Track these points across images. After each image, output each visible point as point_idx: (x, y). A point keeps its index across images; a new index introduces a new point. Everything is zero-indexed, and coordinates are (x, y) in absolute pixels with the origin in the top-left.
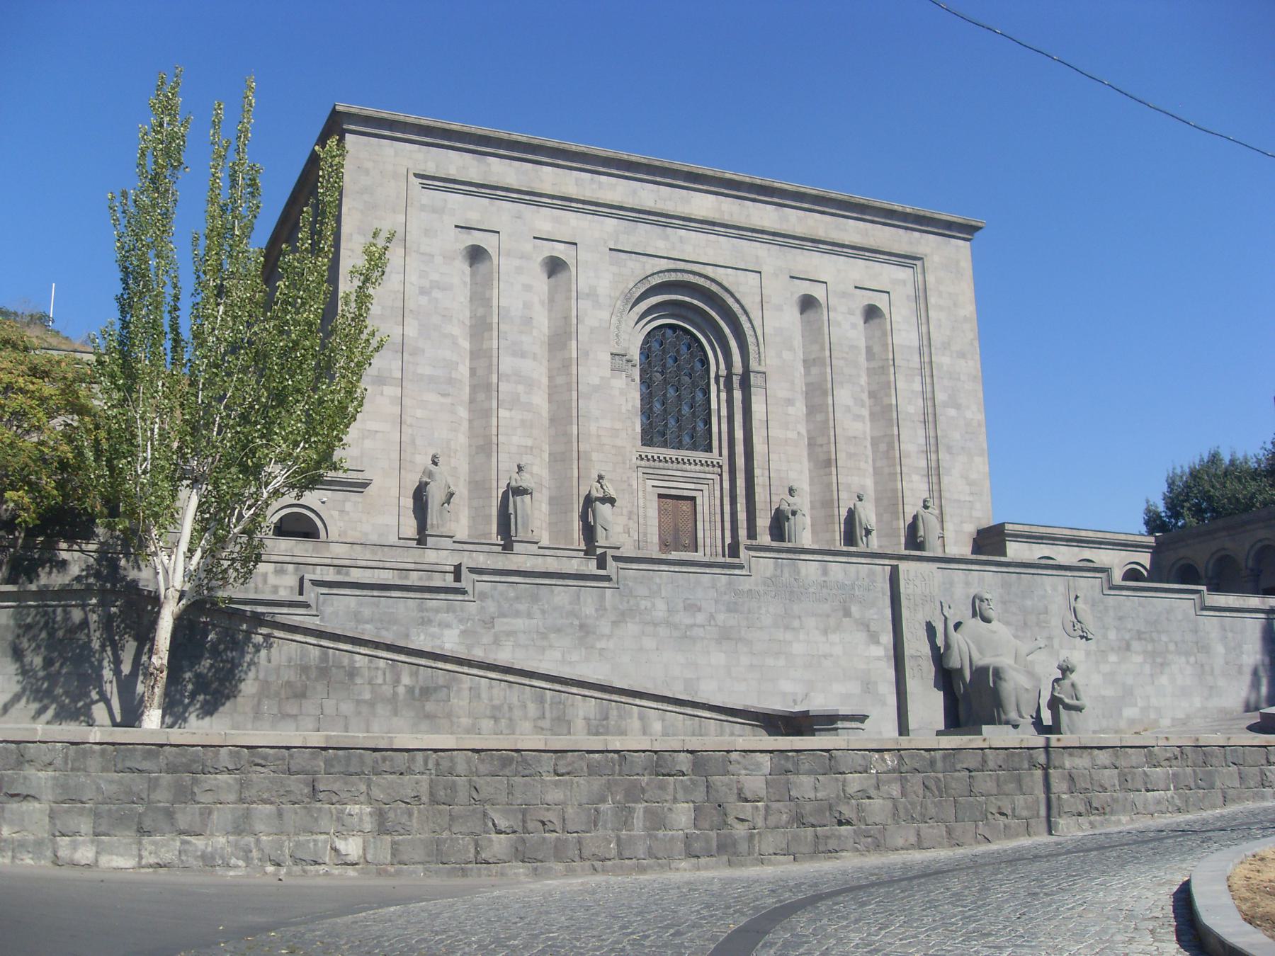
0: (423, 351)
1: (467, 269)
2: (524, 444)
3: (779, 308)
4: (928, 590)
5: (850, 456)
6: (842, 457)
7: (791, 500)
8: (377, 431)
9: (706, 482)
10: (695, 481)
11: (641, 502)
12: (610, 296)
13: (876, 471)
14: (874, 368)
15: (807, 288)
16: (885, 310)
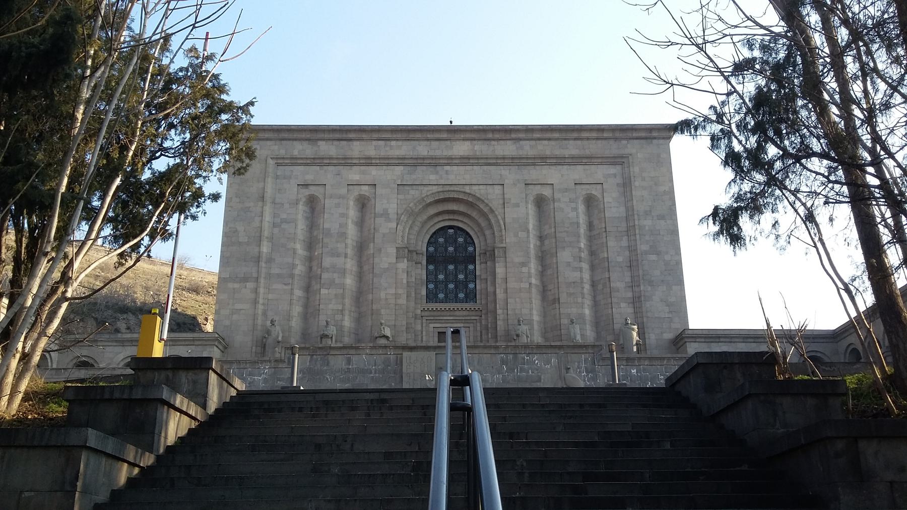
0: (274, 259)
3: (517, 205)
4: (426, 369)
5: (570, 295)
6: (563, 298)
8: (241, 310)
9: (471, 321)
14: (594, 235)
15: (537, 190)
16: (599, 196)
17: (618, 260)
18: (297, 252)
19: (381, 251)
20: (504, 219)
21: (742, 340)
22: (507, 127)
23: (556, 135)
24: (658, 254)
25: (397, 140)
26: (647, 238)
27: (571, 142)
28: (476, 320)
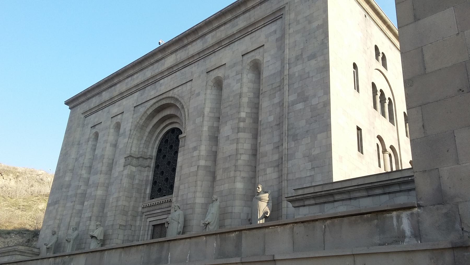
3: (198, 94)
8: (50, 225)
17: (269, 121)
18: (82, 177)
20: (188, 110)
21: (365, 194)
22: (193, 29)
23: (229, 17)
24: (305, 101)
25: (137, 73)
26: (296, 86)
27: (242, 17)
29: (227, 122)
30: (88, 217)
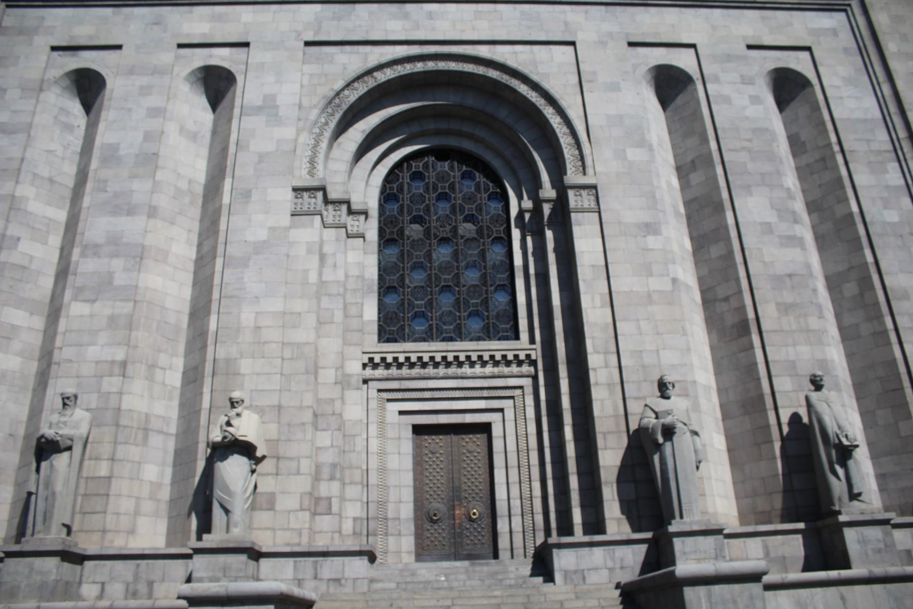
1: (76, 107)
2: (109, 359)
3: (614, 87)
5: (785, 308)
7: (662, 405)
10: (485, 393)
11: (374, 444)
12: (300, 106)
13: (847, 335)
14: (808, 165)
16: (811, 75)
19: (250, 197)
28: (521, 387)
29: (749, 187)
30: (106, 362)
